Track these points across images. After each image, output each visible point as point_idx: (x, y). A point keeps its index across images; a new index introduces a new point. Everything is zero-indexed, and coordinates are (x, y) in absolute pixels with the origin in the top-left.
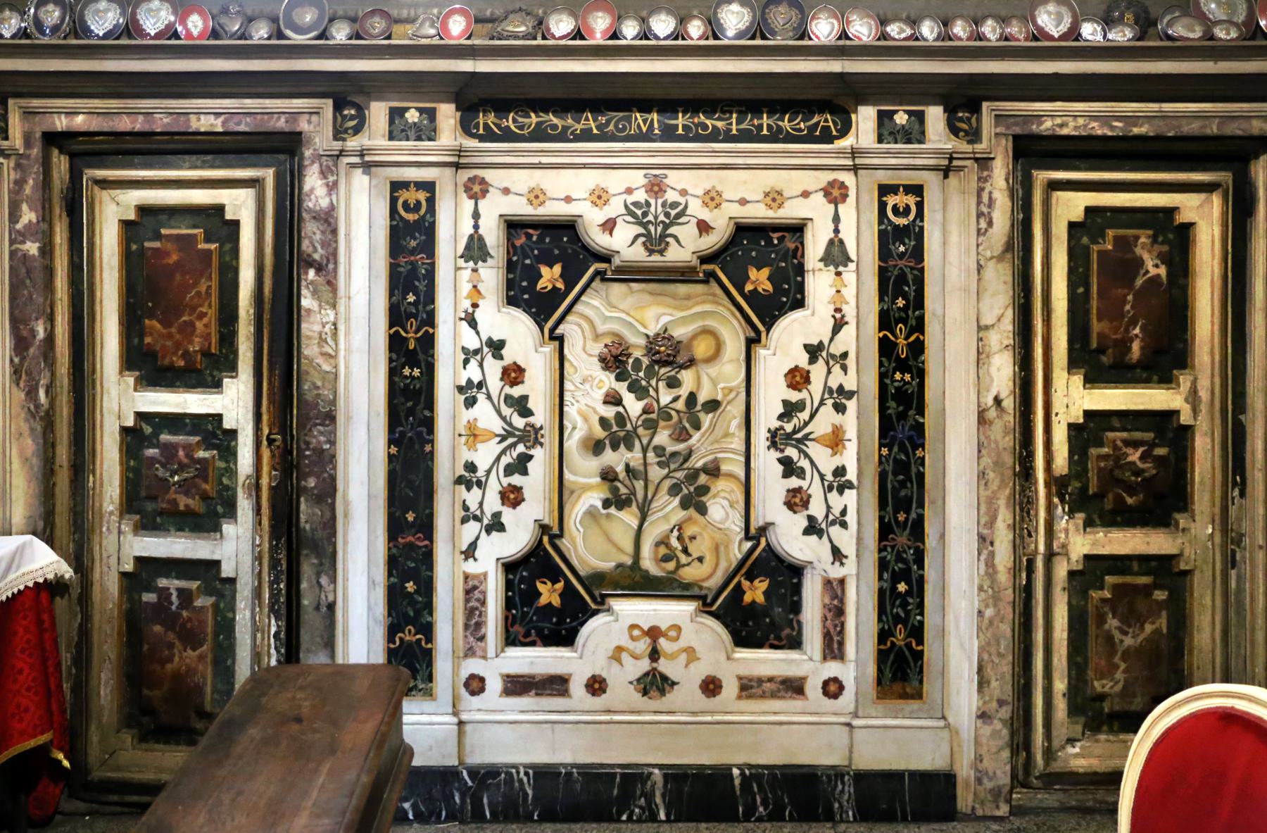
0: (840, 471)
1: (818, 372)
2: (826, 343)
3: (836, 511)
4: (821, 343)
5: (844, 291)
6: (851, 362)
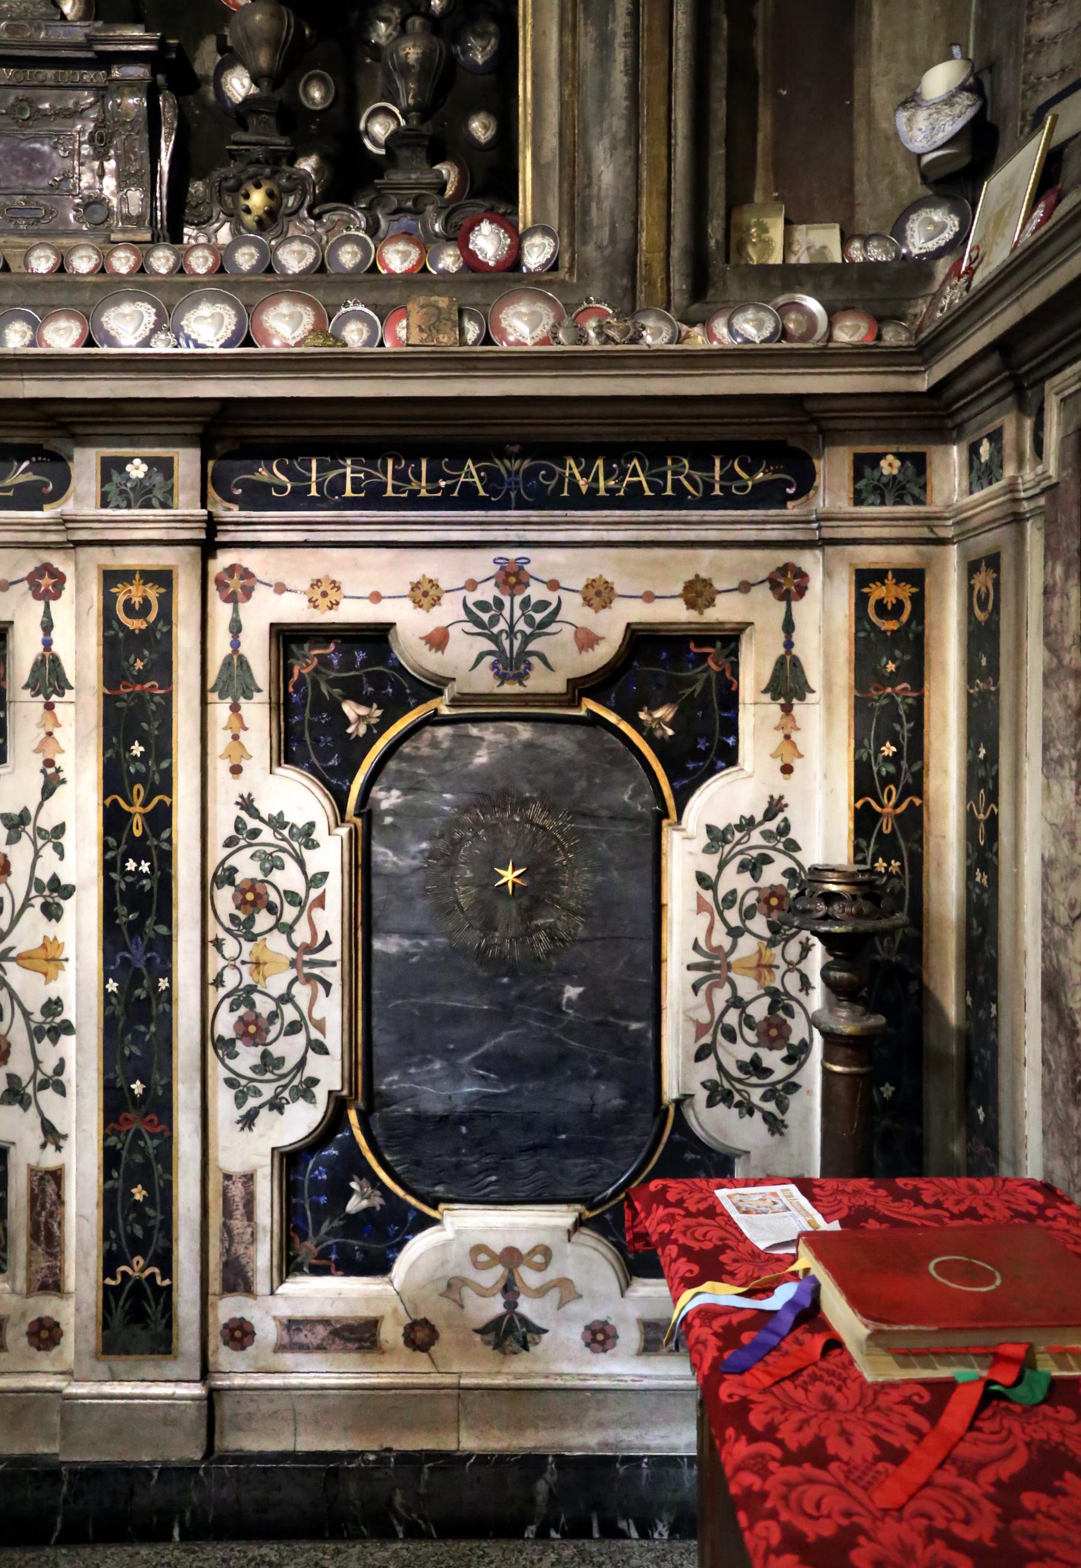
0: (53, 1006)
2: (33, 812)
3: (48, 1068)
5: (57, 733)
6: (66, 840)
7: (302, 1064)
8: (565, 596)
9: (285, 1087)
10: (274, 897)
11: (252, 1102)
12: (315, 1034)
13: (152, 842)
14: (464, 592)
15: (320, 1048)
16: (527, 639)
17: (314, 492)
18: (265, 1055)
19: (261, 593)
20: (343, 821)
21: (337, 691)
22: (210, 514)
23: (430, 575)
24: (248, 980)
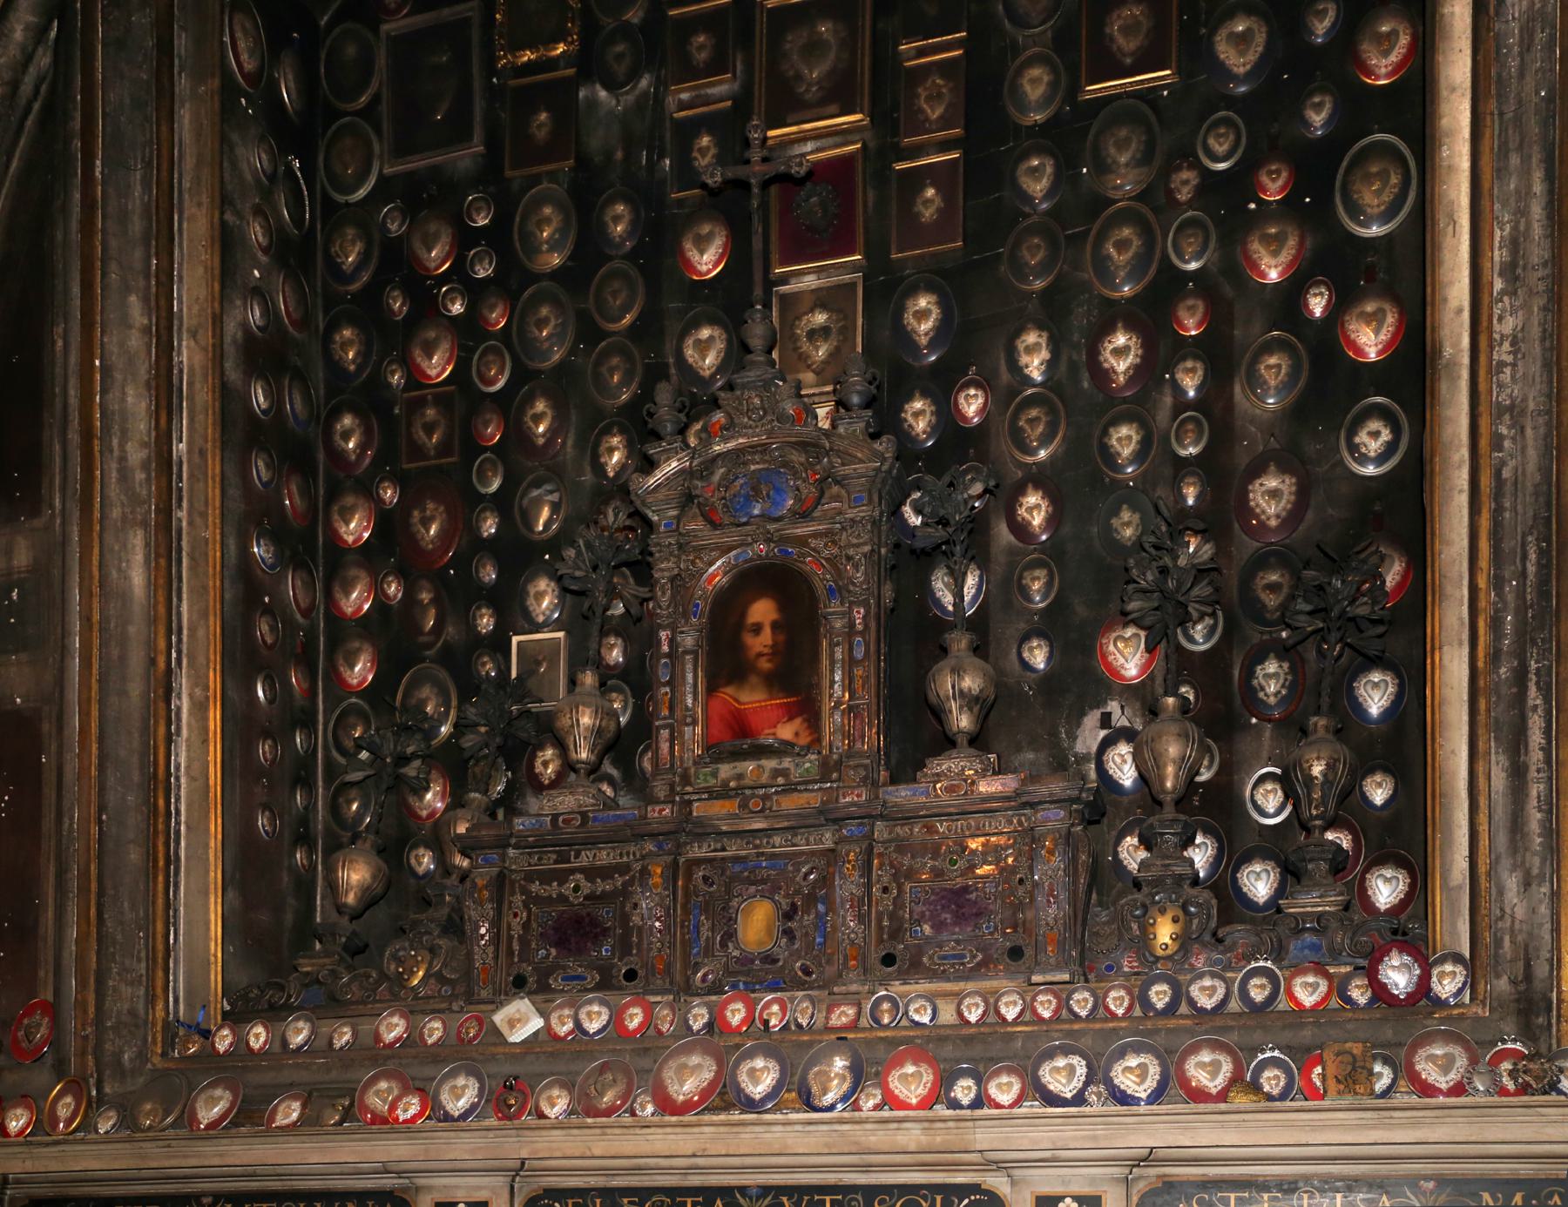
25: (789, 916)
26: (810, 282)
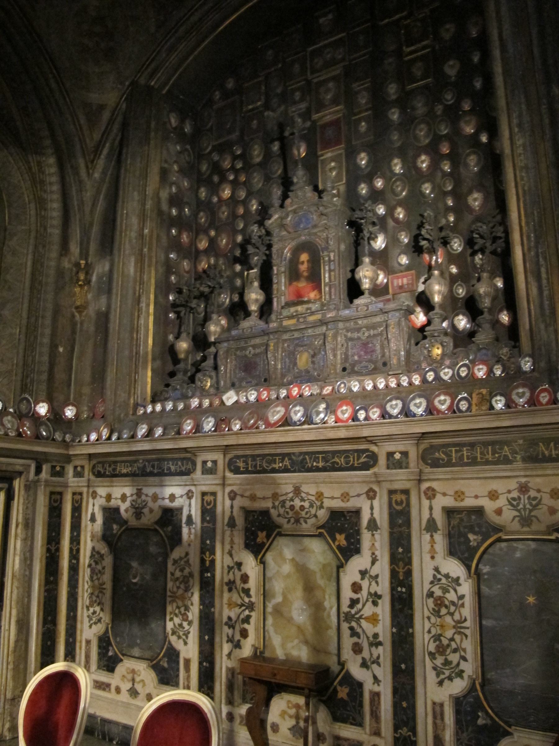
0: (376, 636)
1: (365, 584)
2: (368, 569)
3: (375, 656)
4: (366, 570)
6: (379, 580)
7: (458, 664)
8: (544, 495)
9: (453, 672)
10: (447, 603)
11: (442, 677)
12: (463, 654)
13: (406, 581)
14: (506, 495)
15: (465, 659)
16: (531, 511)
17: (454, 461)
18: (446, 660)
19: (438, 496)
20: (470, 576)
21: (466, 530)
22: (421, 470)
23: (495, 489)
24: (439, 632)
25: (313, 356)
26: (329, 155)
